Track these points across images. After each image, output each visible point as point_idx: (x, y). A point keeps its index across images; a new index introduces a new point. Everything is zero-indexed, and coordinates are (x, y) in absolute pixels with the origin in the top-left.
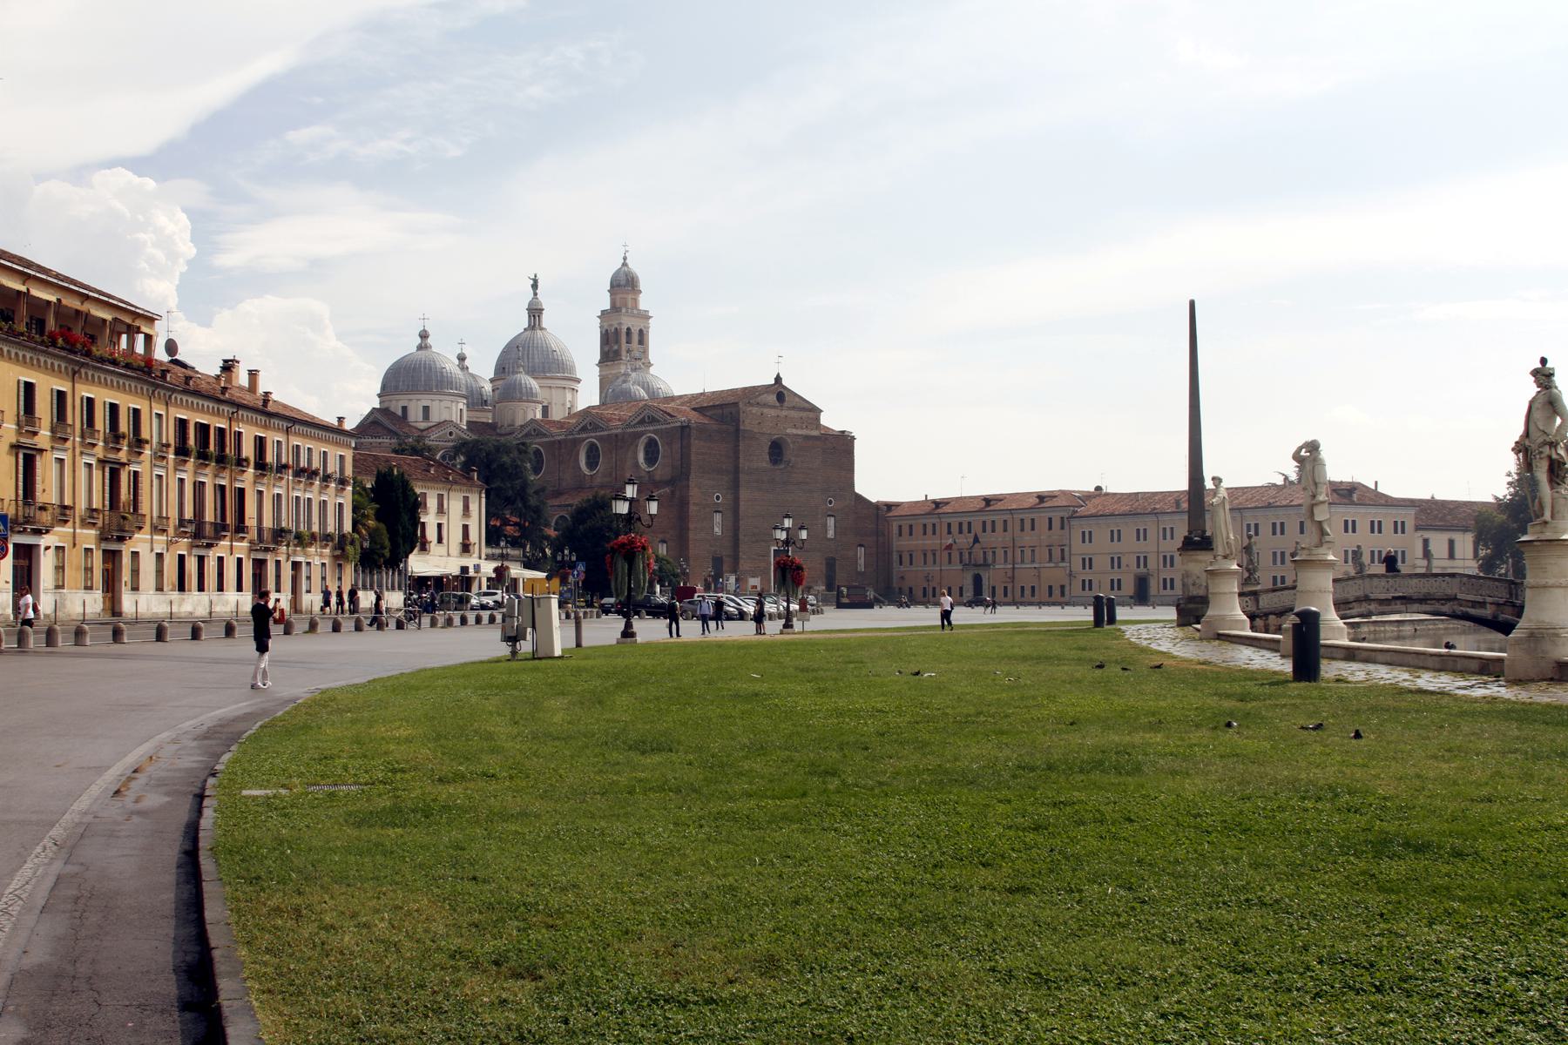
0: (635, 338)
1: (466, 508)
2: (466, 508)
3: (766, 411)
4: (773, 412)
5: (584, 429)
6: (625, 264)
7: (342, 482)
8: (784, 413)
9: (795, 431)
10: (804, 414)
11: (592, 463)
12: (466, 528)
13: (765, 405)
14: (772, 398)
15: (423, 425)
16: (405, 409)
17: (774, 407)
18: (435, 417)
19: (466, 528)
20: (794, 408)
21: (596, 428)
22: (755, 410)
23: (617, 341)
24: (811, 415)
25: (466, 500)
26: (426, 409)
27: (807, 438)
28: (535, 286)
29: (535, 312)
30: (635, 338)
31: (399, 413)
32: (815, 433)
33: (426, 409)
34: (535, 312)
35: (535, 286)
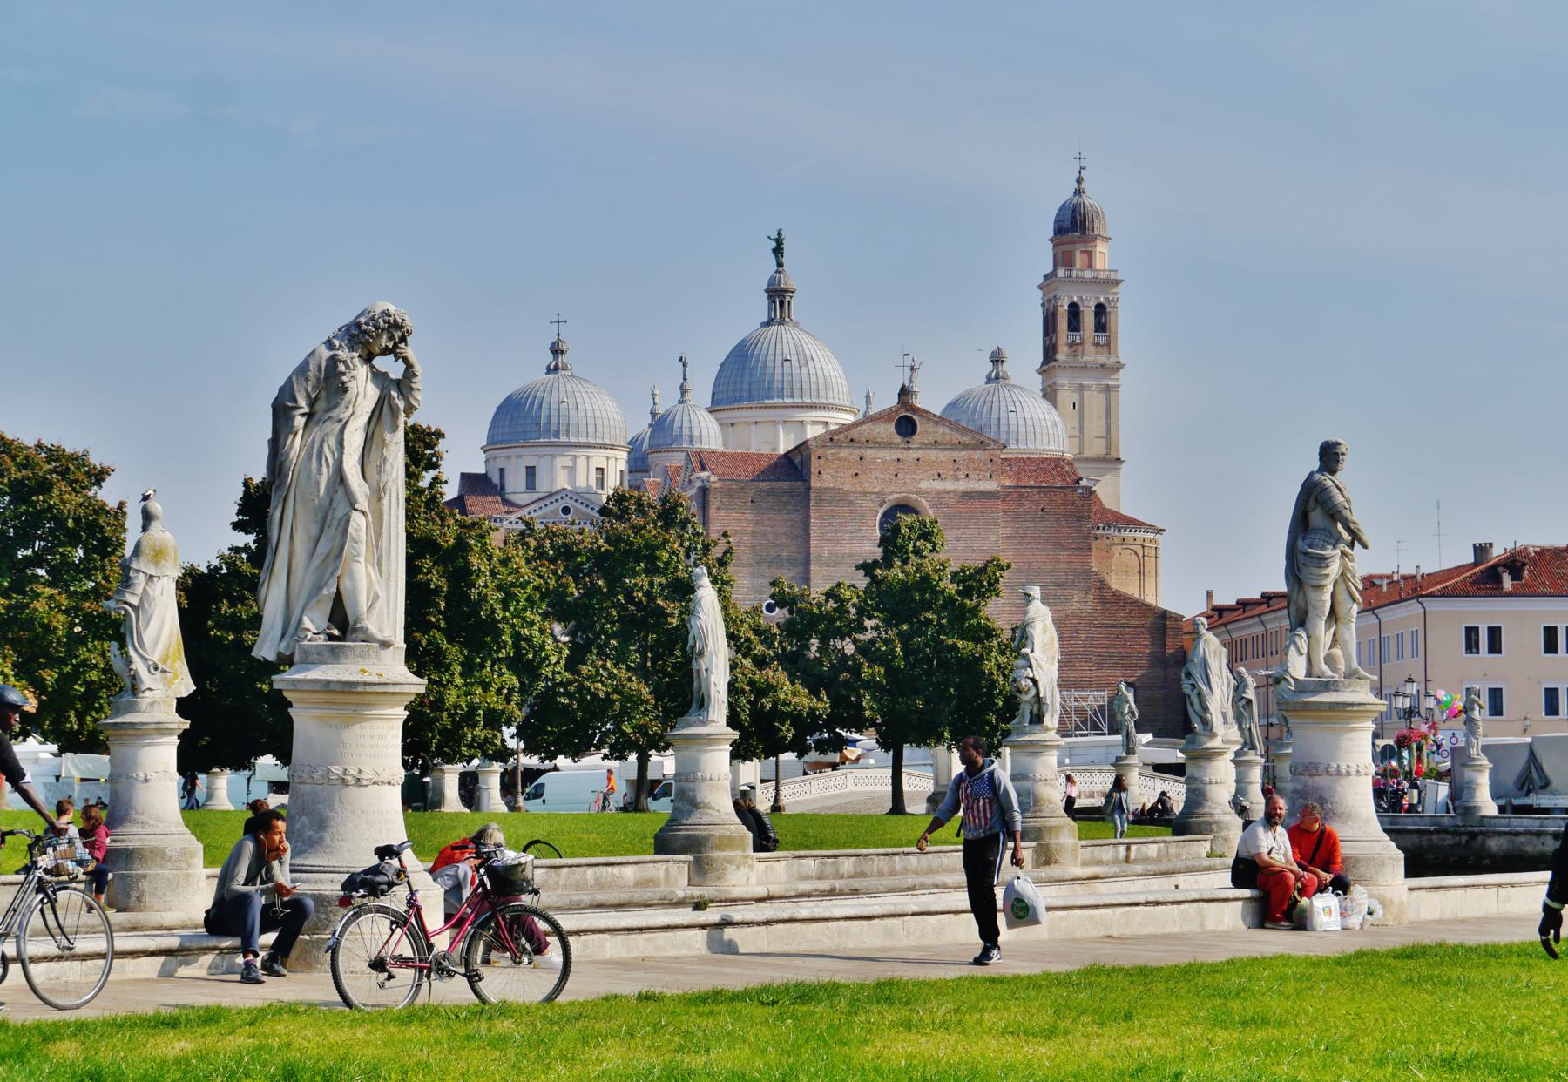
0: (1088, 319)
3: (868, 453)
4: (889, 455)
6: (1078, 192)
8: (913, 455)
9: (938, 485)
10: (961, 455)
14: (888, 430)
16: (502, 471)
17: (889, 445)
18: (543, 486)
22: (844, 453)
23: (1055, 330)
24: (978, 455)
26: (531, 471)
27: (968, 495)
28: (778, 251)
29: (778, 296)
30: (1088, 319)
33: (531, 471)
34: (778, 296)
35: (778, 251)
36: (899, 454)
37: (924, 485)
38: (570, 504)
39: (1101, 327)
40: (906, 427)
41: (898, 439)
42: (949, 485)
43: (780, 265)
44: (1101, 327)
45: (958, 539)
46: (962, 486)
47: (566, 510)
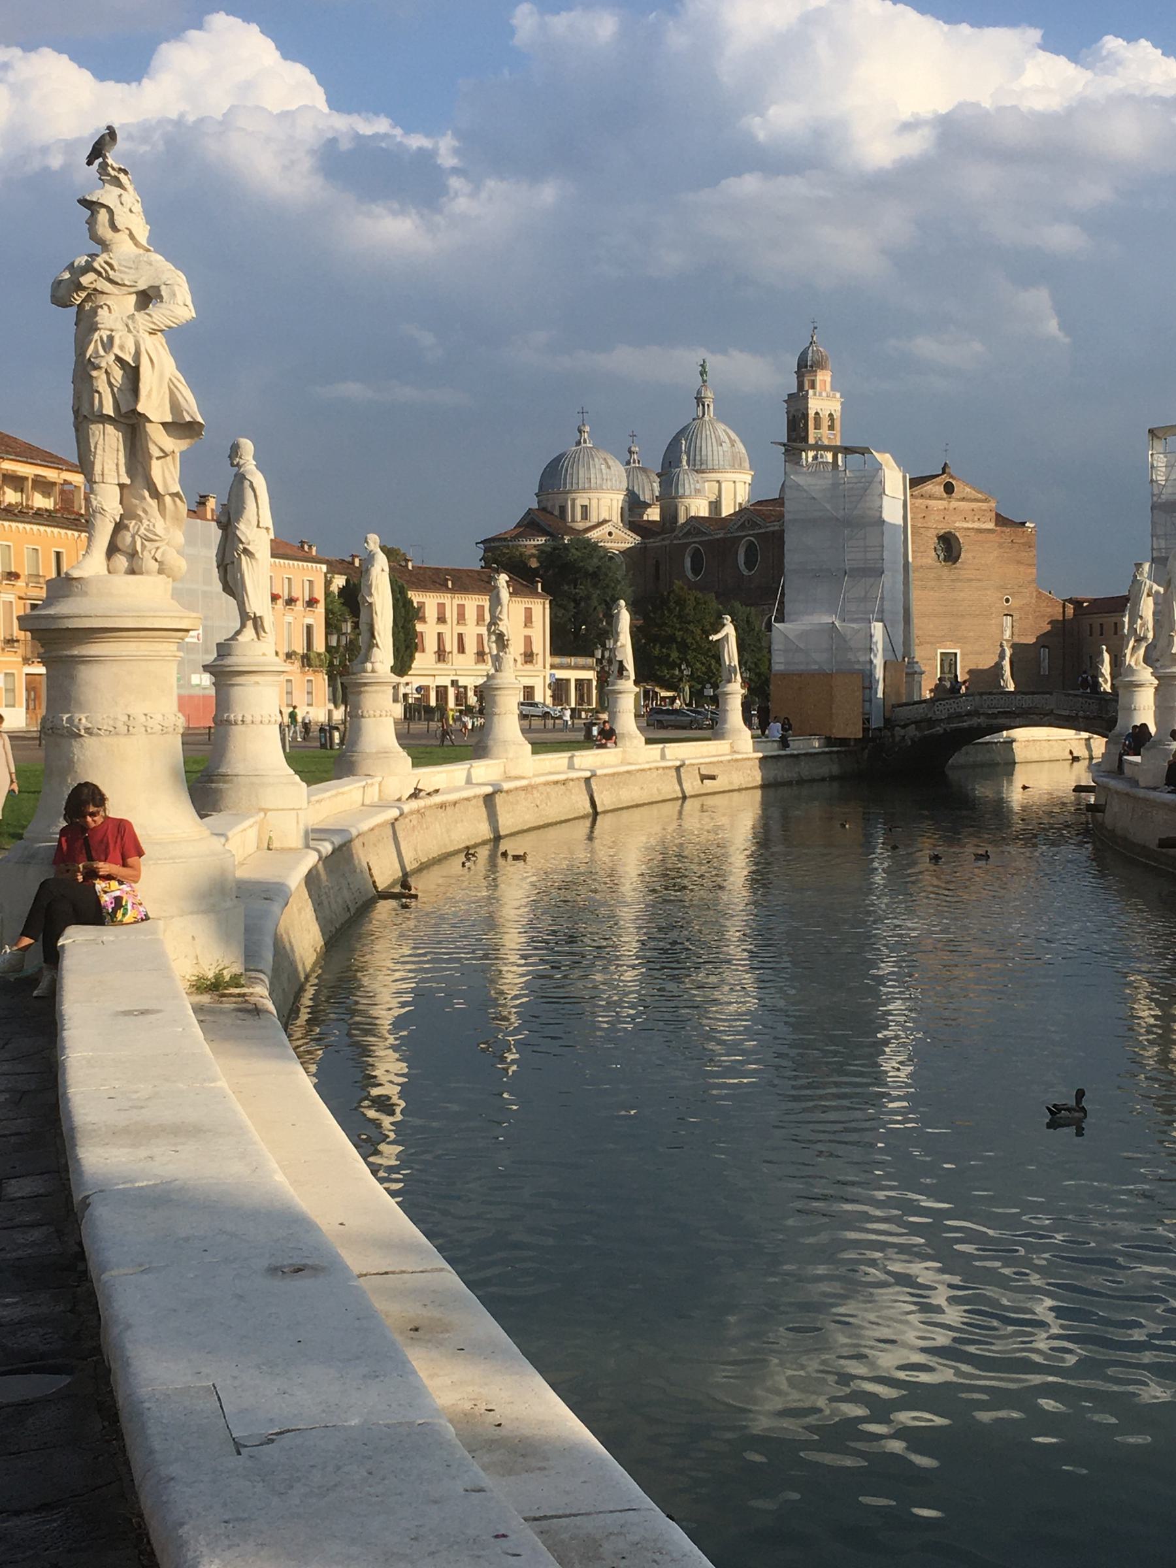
0: (825, 423)
1: (528, 621)
2: (528, 621)
3: (931, 503)
5: (742, 527)
7: (312, 602)
8: (954, 504)
9: (966, 525)
10: (975, 505)
11: (750, 564)
12: (528, 640)
13: (930, 497)
15: (580, 525)
17: (941, 499)
19: (528, 640)
20: (963, 499)
21: (755, 525)
24: (984, 506)
25: (528, 611)
27: (979, 531)
30: (825, 423)
31: (557, 513)
32: (991, 525)
33: (585, 508)
36: (945, 503)
37: (957, 525)
38: (613, 530)
39: (831, 428)
40: (949, 489)
41: (945, 495)
42: (970, 525)
43: (704, 381)
44: (831, 428)
45: (974, 558)
46: (976, 525)
47: (610, 534)
